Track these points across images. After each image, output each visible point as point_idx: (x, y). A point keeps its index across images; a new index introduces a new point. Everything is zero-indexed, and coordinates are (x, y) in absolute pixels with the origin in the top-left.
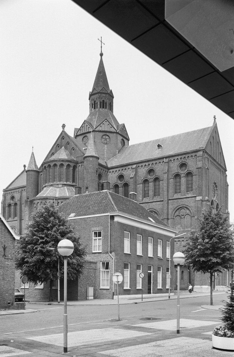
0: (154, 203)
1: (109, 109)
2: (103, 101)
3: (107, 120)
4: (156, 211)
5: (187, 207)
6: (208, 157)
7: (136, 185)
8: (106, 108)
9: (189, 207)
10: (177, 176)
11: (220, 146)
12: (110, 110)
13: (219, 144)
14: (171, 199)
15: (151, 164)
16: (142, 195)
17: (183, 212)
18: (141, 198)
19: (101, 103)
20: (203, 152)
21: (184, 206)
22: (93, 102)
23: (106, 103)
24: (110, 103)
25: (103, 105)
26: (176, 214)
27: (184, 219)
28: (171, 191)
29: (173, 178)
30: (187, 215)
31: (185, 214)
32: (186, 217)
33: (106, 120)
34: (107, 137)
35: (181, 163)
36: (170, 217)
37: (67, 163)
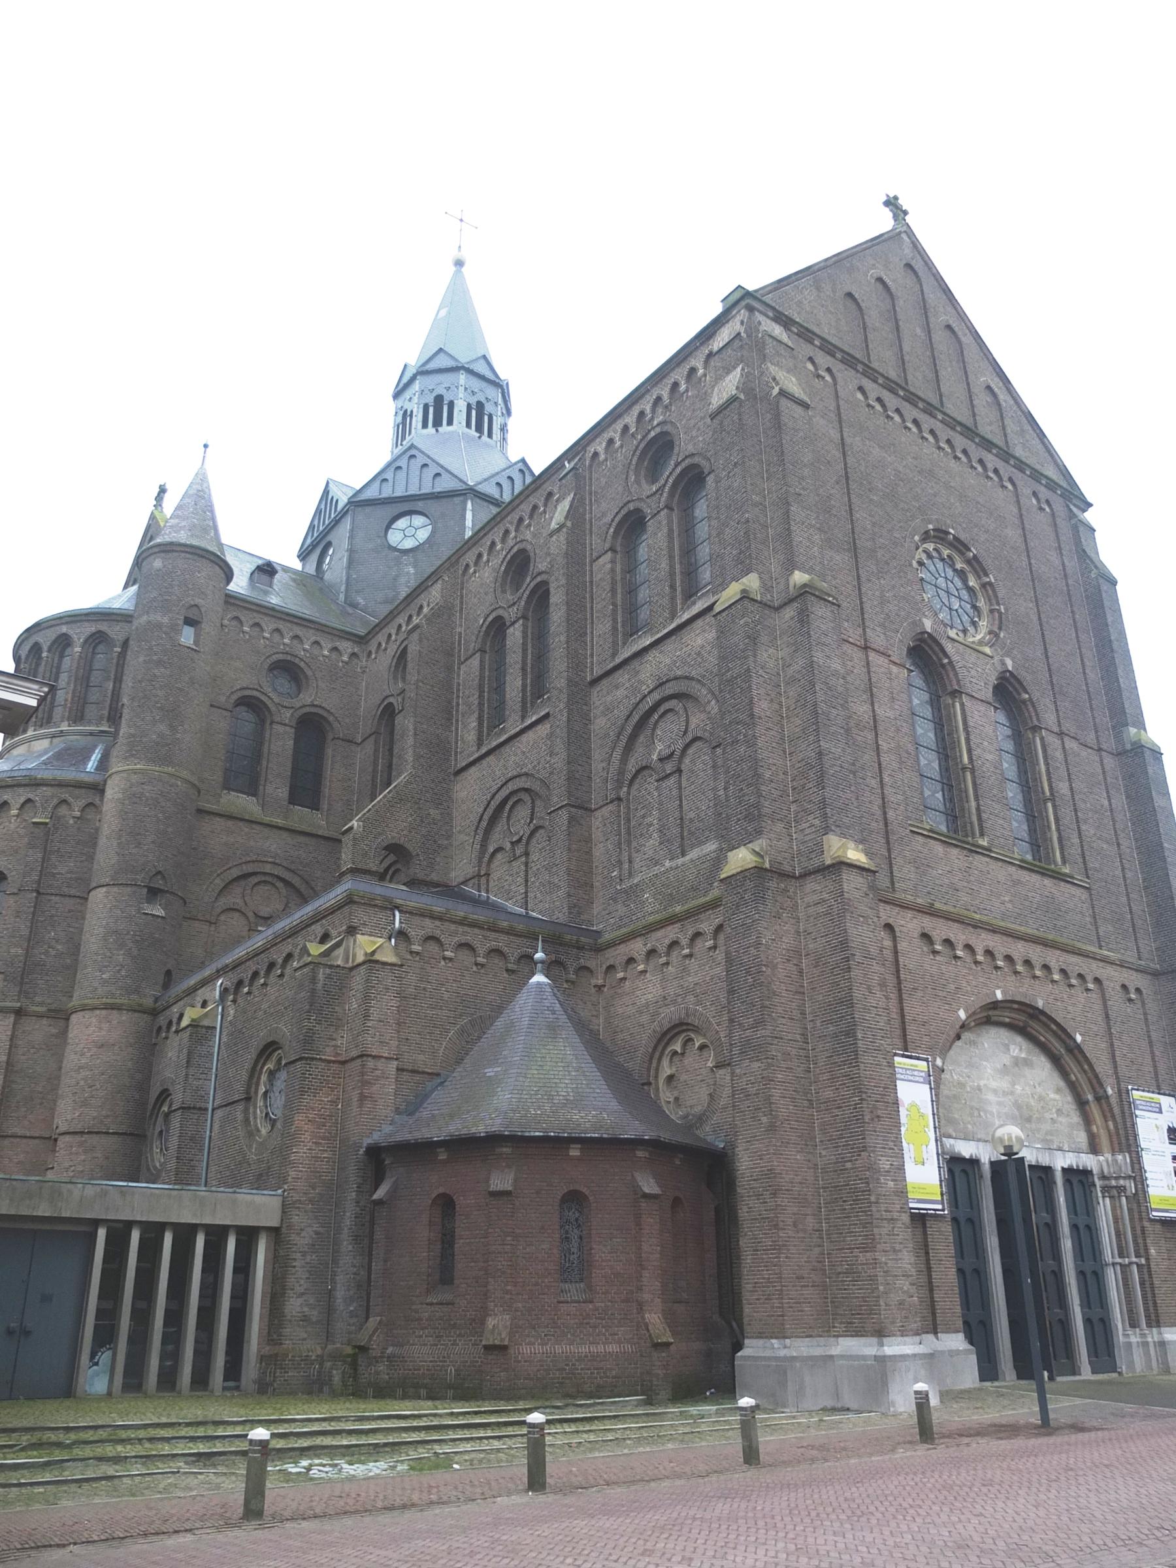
0: (524, 738)
1: (468, 425)
2: (439, 399)
3: (416, 448)
4: (536, 786)
5: (682, 687)
6: (823, 360)
7: (449, 668)
8: (450, 423)
9: (698, 686)
10: (632, 524)
11: (971, 352)
12: (479, 429)
13: (967, 339)
14: (598, 671)
15: (512, 529)
16: (476, 715)
17: (665, 738)
18: (471, 737)
19: (426, 407)
20: (751, 309)
21: (669, 689)
22: (399, 419)
23: (451, 405)
24: (480, 405)
25: (438, 411)
26: (632, 767)
27: (672, 780)
28: (602, 628)
29: (607, 546)
30: (690, 751)
31: (680, 745)
32: (687, 761)
33: (413, 452)
34: (418, 520)
35: (642, 446)
36: (595, 799)
37: (90, 628)
